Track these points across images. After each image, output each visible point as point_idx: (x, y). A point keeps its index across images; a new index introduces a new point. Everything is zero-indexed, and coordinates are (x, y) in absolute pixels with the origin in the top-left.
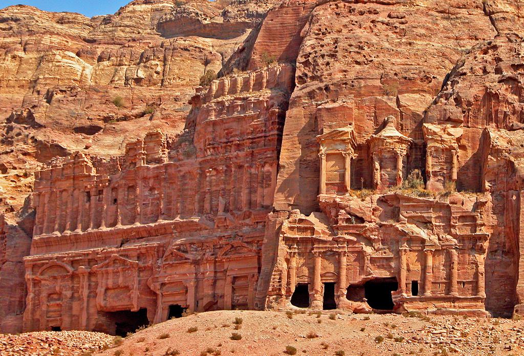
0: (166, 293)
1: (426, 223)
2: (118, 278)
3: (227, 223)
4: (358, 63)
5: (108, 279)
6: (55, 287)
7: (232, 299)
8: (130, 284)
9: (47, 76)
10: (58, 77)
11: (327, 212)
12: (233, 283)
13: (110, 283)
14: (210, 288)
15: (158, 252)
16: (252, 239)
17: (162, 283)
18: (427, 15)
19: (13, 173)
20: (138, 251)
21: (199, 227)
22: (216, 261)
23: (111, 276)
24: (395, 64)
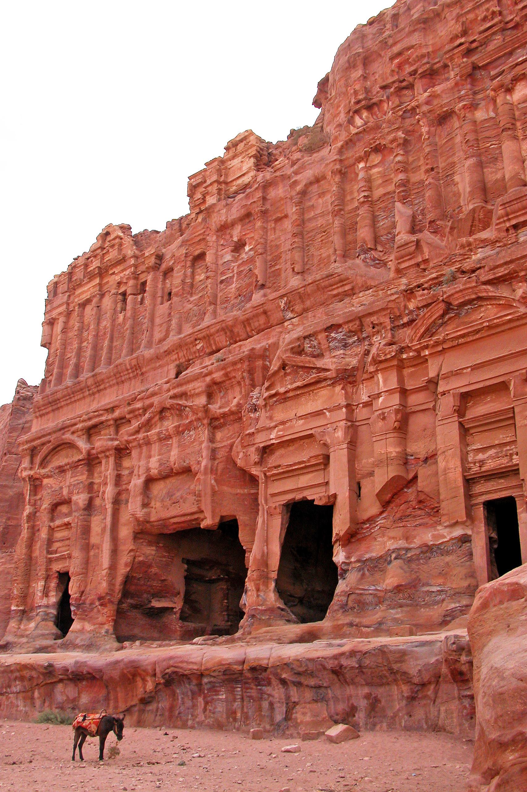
0: (275, 472)
2: (170, 451)
3: (422, 253)
5: (150, 457)
6: (61, 488)
7: (464, 460)
8: (191, 462)
12: (460, 412)
13: (154, 464)
14: (392, 438)
15: (251, 372)
16: (512, 266)
17: (265, 448)
20: (208, 379)
21: (347, 288)
22: (402, 360)
23: (155, 448)
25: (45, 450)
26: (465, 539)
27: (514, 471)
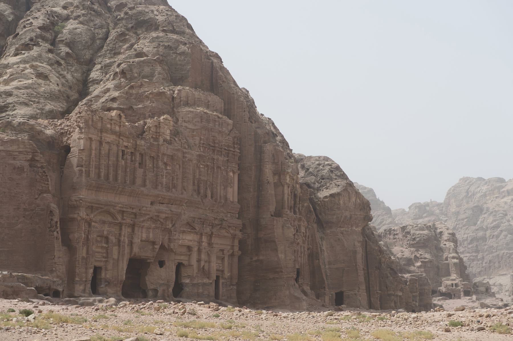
20: (167, 215)
23: (144, 230)
25: (100, 210)
26: (211, 283)
27: (223, 271)
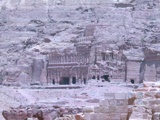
1: (113, 67)
4: (103, 38)
9: (37, 3)
10: (40, 3)
11: (98, 64)
18: (115, 28)
19: (41, 45)
24: (109, 38)
